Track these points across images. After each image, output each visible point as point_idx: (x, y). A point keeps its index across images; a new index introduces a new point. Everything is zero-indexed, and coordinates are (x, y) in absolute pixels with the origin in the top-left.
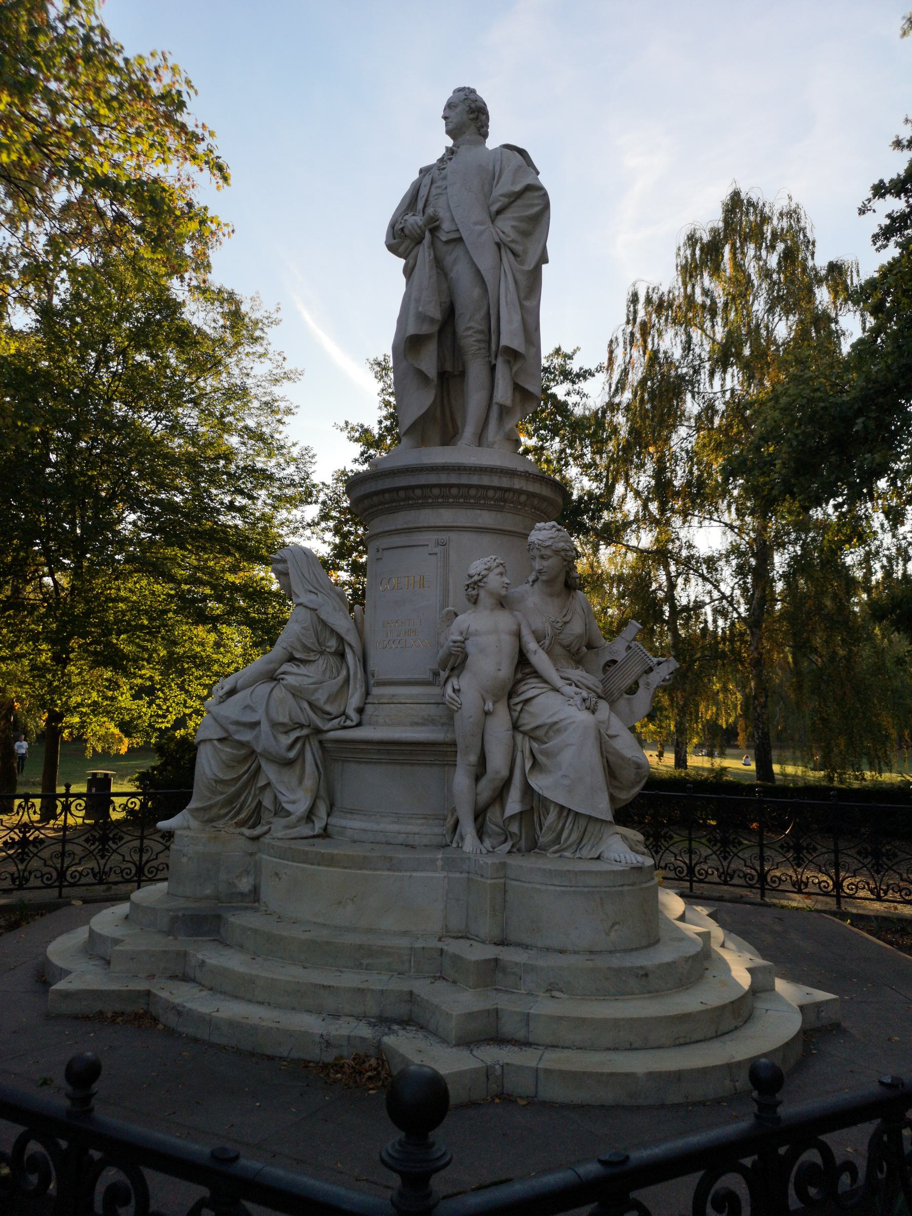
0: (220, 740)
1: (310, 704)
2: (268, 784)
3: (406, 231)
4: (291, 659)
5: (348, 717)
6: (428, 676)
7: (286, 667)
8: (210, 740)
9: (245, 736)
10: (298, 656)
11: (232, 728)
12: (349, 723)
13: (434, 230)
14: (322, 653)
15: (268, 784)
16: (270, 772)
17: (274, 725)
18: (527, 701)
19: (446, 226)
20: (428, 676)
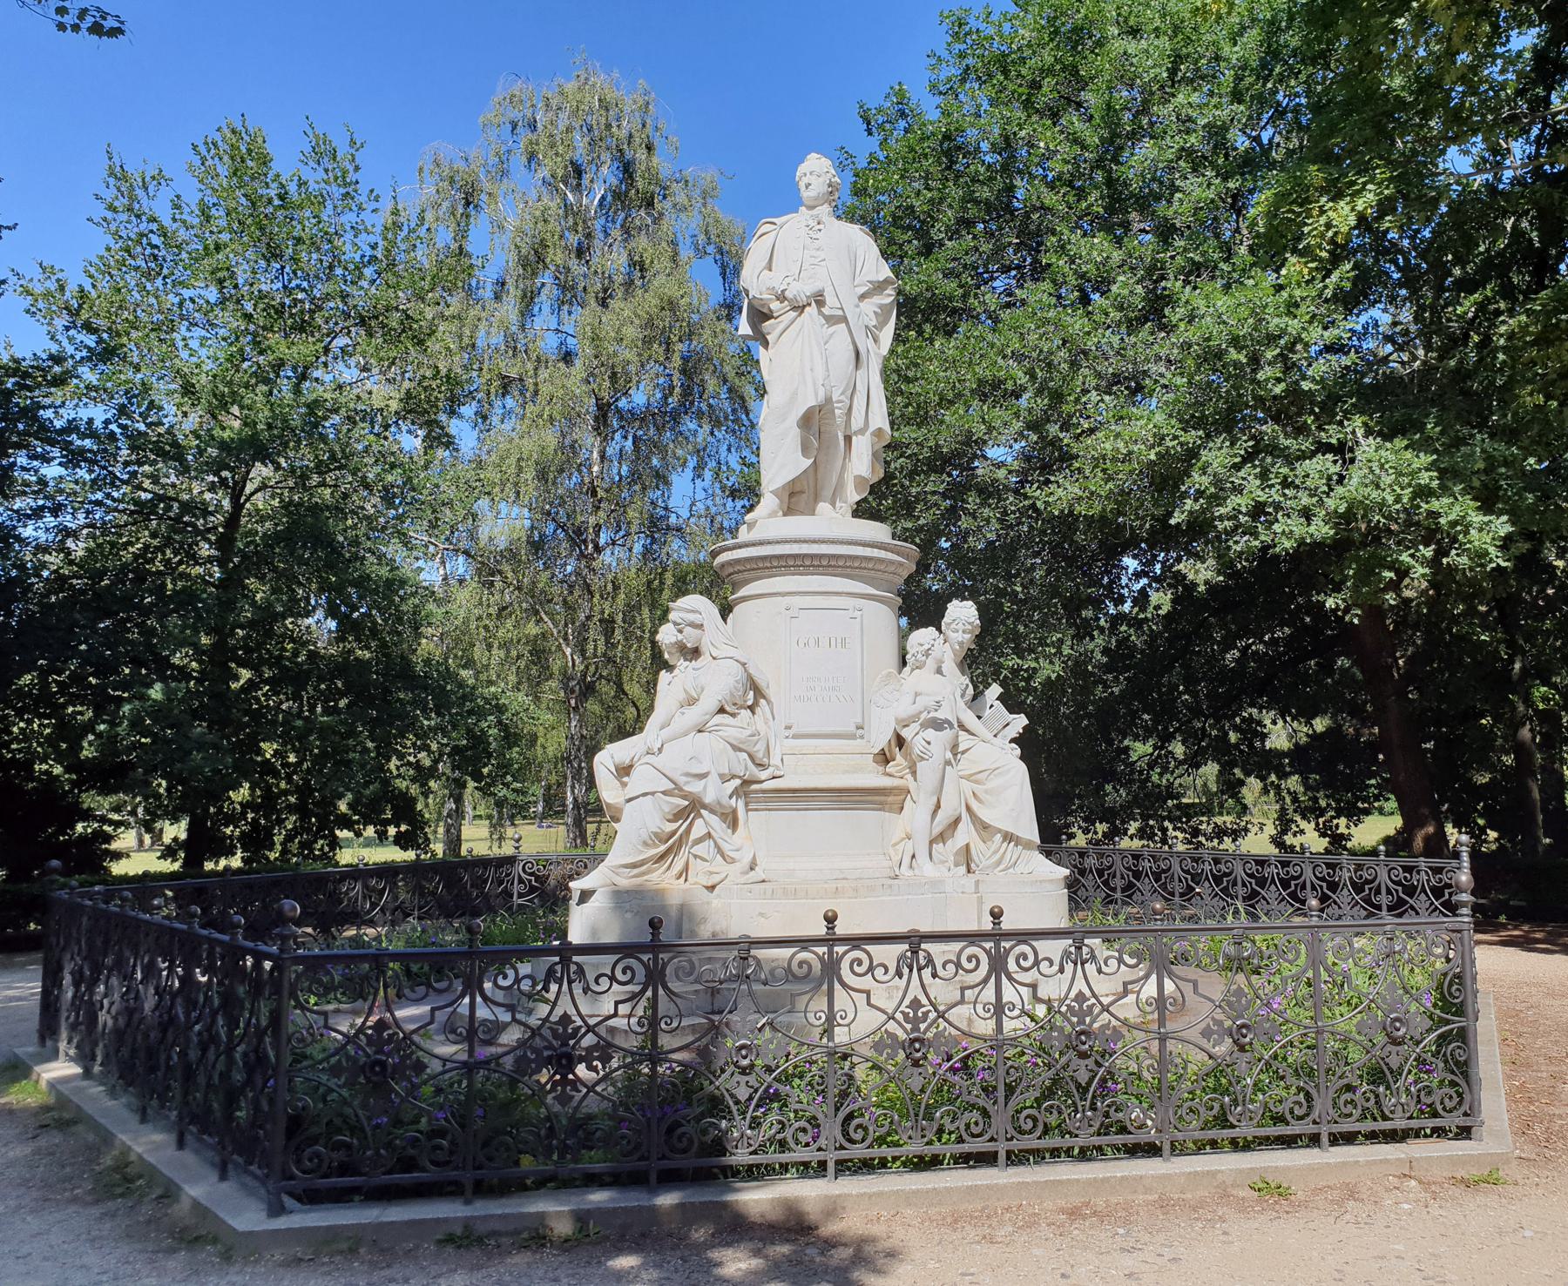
0: (664, 793)
1: (750, 756)
2: (709, 835)
3: (787, 294)
4: (722, 711)
5: (777, 768)
6: (852, 729)
7: (720, 718)
8: (653, 794)
9: (694, 787)
10: (727, 708)
11: (681, 780)
12: (778, 773)
13: (820, 303)
14: (741, 707)
15: (709, 835)
16: (714, 820)
17: (721, 776)
18: (963, 753)
19: (830, 300)
20: (852, 729)
